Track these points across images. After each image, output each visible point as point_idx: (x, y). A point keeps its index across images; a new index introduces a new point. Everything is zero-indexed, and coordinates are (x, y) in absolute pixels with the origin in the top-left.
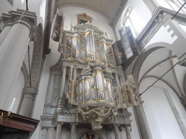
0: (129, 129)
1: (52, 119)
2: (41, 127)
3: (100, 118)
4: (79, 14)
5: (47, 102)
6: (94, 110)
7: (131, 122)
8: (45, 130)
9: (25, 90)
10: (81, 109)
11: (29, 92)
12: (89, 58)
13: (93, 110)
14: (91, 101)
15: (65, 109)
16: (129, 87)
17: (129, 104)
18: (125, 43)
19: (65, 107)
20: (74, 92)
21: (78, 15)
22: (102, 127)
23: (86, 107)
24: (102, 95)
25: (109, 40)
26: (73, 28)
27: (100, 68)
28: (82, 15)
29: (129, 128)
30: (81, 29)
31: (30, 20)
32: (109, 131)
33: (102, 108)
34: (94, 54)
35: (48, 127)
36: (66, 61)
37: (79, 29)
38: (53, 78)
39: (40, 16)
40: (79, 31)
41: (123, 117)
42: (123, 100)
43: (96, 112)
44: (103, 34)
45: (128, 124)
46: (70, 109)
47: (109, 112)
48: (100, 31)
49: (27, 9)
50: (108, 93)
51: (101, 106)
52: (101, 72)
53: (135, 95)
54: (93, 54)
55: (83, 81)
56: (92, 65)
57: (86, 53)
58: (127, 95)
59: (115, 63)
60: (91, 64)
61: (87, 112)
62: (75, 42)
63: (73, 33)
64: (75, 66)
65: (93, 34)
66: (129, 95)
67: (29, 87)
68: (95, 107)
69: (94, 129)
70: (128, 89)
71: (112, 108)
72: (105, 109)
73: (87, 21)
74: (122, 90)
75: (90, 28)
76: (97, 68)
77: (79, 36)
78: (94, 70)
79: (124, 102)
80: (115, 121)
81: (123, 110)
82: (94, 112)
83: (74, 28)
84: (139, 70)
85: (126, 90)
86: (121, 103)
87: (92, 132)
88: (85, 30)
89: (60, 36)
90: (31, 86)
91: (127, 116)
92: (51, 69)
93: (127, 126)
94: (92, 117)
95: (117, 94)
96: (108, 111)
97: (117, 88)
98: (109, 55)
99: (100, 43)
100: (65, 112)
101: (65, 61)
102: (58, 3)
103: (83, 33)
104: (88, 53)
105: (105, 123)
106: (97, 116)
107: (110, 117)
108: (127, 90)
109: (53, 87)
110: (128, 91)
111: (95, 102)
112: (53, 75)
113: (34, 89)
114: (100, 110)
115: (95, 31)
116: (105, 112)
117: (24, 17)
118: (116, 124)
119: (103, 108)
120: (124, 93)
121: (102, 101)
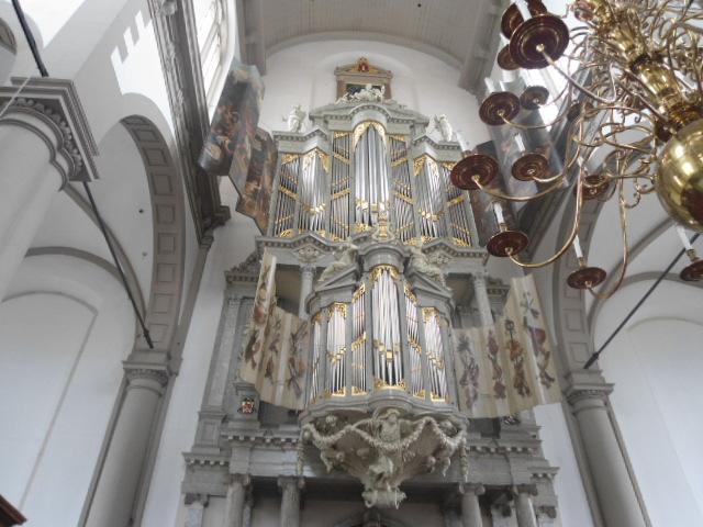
0: (531, 505)
2: (184, 497)
3: (382, 459)
4: (339, 66)
6: (356, 425)
7: (553, 475)
8: (198, 506)
9: (133, 363)
10: (311, 423)
11: (144, 367)
13: (353, 427)
14: (349, 392)
15: (258, 424)
16: (516, 328)
17: (518, 398)
18: (508, 150)
19: (259, 418)
21: (337, 68)
22: (403, 496)
23: (325, 417)
25: (448, 147)
26: (307, 118)
27: (390, 259)
28: (353, 67)
29: (529, 502)
31: (46, 108)
32: (452, 513)
33: (387, 419)
34: (382, 207)
35: (209, 496)
36: (273, 244)
37: (330, 121)
38: (233, 311)
39: (124, 90)
40: (330, 127)
41: (502, 452)
42: (494, 382)
43: (364, 434)
44: (426, 124)
45: (523, 485)
46: (277, 426)
47: (416, 433)
48: (411, 115)
49: (44, 73)
50: (424, 358)
51: (384, 411)
52: (392, 273)
53: (543, 357)
54: (378, 207)
55: (322, 316)
56: (356, 251)
57: (352, 205)
58: (509, 359)
60: (354, 247)
62: (309, 172)
63: (304, 139)
64: (308, 261)
65: (382, 132)
66: (519, 359)
67: (146, 351)
69: (369, 503)
70: (514, 337)
71: (428, 418)
72: (400, 421)
73: (364, 87)
74: (492, 341)
75: (369, 111)
76: (378, 259)
77: (326, 147)
78: (366, 268)
79: (500, 391)
80: (462, 474)
81: (503, 426)
82: (354, 432)
83: (311, 118)
85: (507, 339)
86: (488, 396)
87: (379, 516)
89: (236, 153)
90: (151, 347)
91: (519, 450)
92: (231, 280)
93: (520, 491)
94: (355, 454)
95: (472, 359)
96: (414, 428)
97: (471, 334)
98: (449, 204)
99: (411, 163)
100: (257, 438)
101: (267, 244)
102: (252, 39)
103: (343, 132)
104: (359, 205)
105: (419, 480)
106: (373, 455)
107: (434, 455)
108: (509, 338)
109: (234, 346)
110: (514, 345)
111: (364, 393)
113: (162, 358)
114: (380, 427)
115: (393, 119)
116: (403, 435)
117: (23, 101)
118: (469, 484)
119: (393, 419)
120: (498, 354)
121: (390, 387)
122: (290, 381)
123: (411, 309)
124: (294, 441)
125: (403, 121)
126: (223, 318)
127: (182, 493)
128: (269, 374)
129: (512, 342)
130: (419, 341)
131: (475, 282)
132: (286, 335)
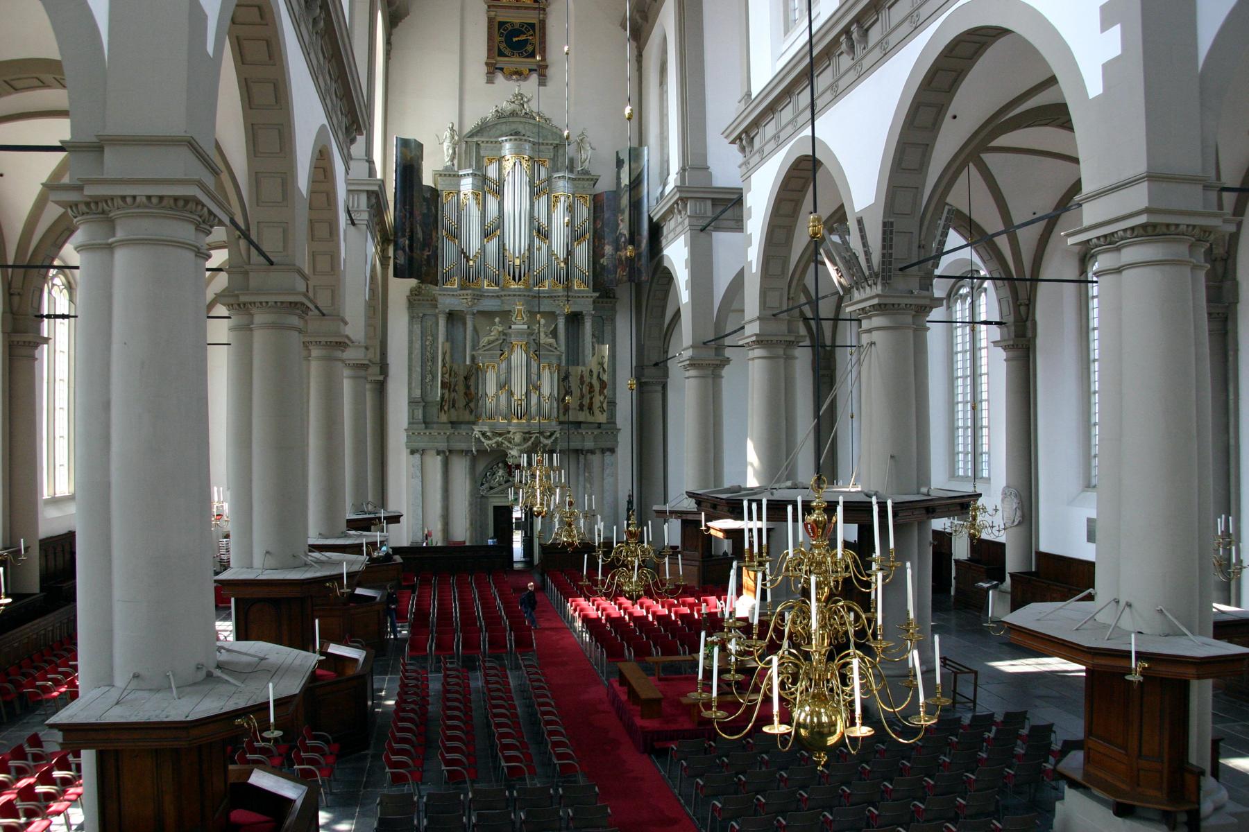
2: (409, 450)
5: (413, 396)
8: (417, 456)
12: (508, 277)
13: (500, 439)
20: (465, 393)
24: (519, 408)
30: (487, 142)
35: (423, 450)
37: (482, 145)
38: (417, 329)
47: (530, 442)
59: (591, 274)
79: (581, 407)
85: (589, 380)
86: (575, 409)
96: (531, 437)
101: (440, 295)
122: (465, 406)
123: (534, 364)
125: (547, 144)
126: (411, 332)
127: (407, 448)
128: (454, 406)
129: (591, 383)
130: (538, 388)
131: (586, 317)
132: (462, 378)
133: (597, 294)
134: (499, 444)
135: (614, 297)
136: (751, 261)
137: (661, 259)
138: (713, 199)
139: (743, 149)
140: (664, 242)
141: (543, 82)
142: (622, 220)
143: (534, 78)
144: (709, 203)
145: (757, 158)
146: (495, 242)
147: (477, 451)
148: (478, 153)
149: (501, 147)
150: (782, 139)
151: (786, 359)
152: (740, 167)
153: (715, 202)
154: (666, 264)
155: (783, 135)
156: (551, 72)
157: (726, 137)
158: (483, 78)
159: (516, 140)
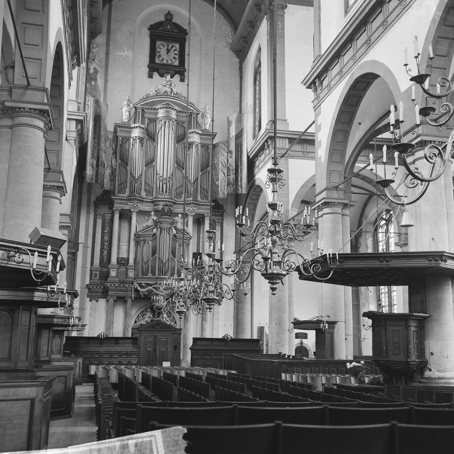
1: (102, 288)
10: (137, 283)
13: (151, 288)
37: (146, 110)
43: (154, 290)
44: (198, 114)
61: (143, 288)
68: (154, 284)
78: (158, 227)
83: (135, 108)
84: (255, 205)
88: (157, 110)
101: (116, 199)
112: (100, 214)
114: (159, 288)
115: (180, 112)
124: (131, 286)
131: (206, 218)
133: (213, 204)
134: (150, 292)
135: (223, 209)
136: (321, 156)
137: (254, 182)
138: (289, 138)
139: (315, 90)
140: (256, 170)
141: (182, 80)
142: (230, 157)
143: (177, 77)
144: (287, 141)
145: (326, 91)
146: (151, 170)
147: (135, 298)
148: (143, 115)
149: (157, 113)
150: (344, 73)
151: (343, 215)
152: (312, 102)
153: (291, 140)
154: (257, 183)
155: (344, 71)
156: (186, 74)
157: (304, 85)
158: (146, 75)
159: (167, 108)
